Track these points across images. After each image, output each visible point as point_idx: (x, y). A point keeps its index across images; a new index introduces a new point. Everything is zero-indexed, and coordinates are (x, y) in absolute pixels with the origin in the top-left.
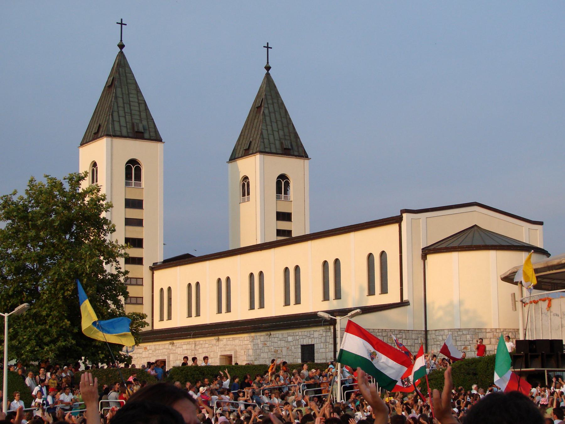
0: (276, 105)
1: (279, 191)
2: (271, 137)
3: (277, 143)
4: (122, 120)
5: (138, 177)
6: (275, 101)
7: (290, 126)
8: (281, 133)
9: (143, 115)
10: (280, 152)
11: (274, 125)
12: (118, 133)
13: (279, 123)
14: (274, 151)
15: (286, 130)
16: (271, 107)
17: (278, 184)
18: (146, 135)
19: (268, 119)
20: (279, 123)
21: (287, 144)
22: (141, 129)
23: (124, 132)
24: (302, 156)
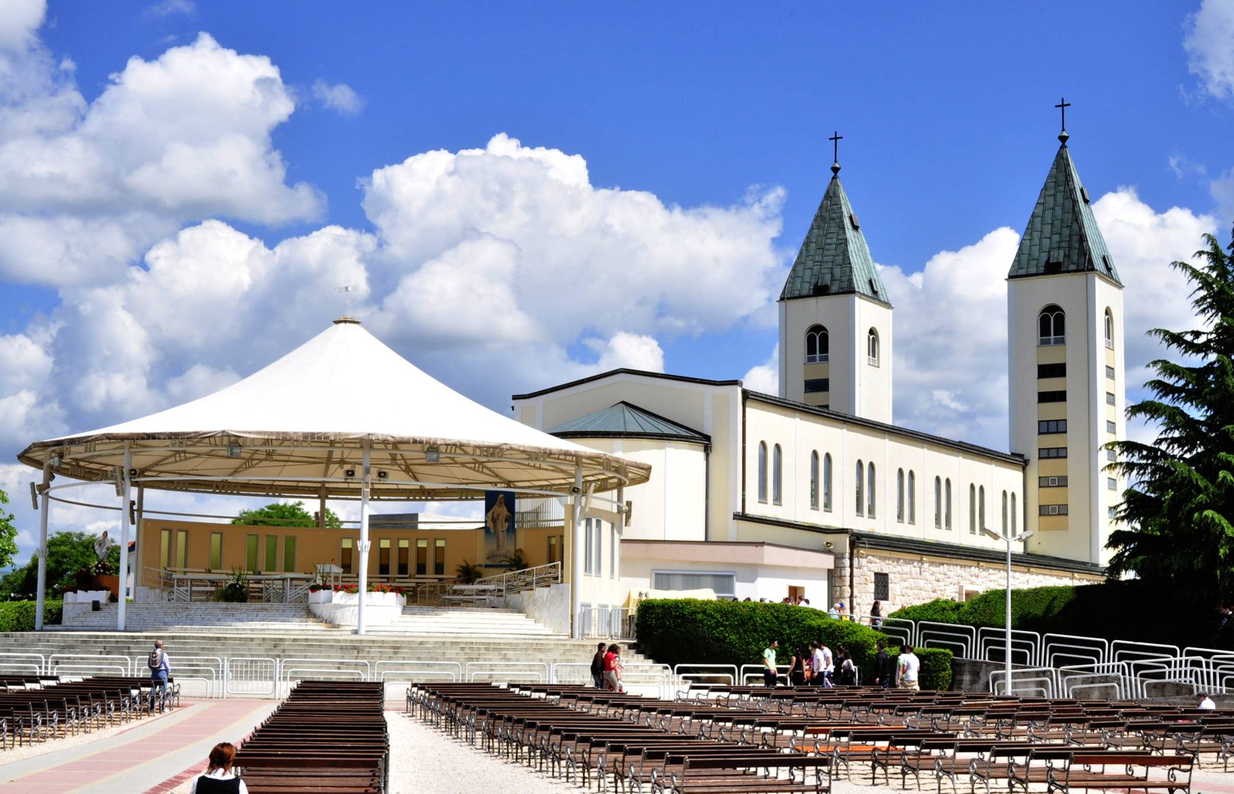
0: (1060, 197)
1: (1044, 331)
2: (1035, 250)
3: (1044, 257)
4: (808, 272)
5: (825, 348)
6: (1061, 188)
7: (1075, 226)
8: (1056, 238)
9: (839, 259)
10: (1042, 269)
11: (1047, 229)
12: (797, 293)
13: (1057, 223)
14: (1033, 271)
15: (1066, 231)
16: (1050, 201)
17: (1044, 322)
18: (834, 288)
19: (1038, 220)
20: (1057, 223)
21: (1058, 256)
22: (827, 280)
23: (805, 292)
24: (1083, 270)
